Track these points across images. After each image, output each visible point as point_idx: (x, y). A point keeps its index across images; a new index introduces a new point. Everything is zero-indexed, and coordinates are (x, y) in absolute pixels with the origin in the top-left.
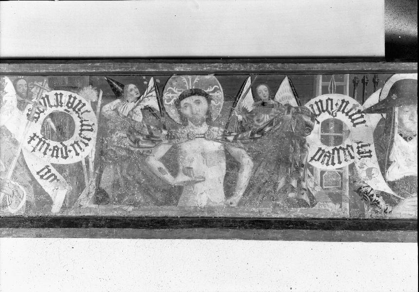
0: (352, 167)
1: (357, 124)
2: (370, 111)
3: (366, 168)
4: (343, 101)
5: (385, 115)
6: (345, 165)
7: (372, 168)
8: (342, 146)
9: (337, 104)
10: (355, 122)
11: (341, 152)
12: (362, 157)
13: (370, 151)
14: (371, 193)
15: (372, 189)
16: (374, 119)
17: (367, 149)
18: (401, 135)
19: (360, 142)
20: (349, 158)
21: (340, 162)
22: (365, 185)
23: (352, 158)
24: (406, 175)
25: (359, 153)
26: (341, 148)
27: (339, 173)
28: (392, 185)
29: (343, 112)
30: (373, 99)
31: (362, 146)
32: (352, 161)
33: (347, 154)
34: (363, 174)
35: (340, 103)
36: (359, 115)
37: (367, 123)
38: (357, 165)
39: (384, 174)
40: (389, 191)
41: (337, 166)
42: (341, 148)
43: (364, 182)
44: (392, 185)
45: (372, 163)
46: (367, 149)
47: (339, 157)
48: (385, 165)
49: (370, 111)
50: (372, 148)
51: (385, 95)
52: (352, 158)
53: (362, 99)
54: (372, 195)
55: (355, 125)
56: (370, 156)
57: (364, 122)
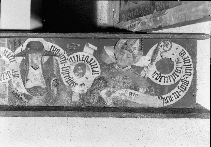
0: (10, 82)
1: (12, 61)
2: (18, 55)
3: (16, 82)
4: (5, 51)
5: (24, 58)
6: (7, 81)
7: (19, 82)
8: (5, 71)
9: (2, 52)
10: (11, 60)
11: (5, 74)
12: (15, 77)
13: (18, 74)
14: (19, 94)
15: (19, 92)
16: (20, 59)
17: (17, 73)
18: (32, 67)
19: (14, 70)
20: (8, 77)
21: (4, 80)
22: (16, 90)
23: (10, 77)
24: (35, 86)
25: (13, 75)
26: (4, 73)
27: (4, 84)
28: (29, 90)
29: (5, 56)
30: (19, 50)
31: (15, 72)
32: (9, 79)
33: (8, 75)
34: (15, 85)
35: (3, 52)
36: (13, 57)
37: (16, 61)
38: (12, 81)
39: (25, 86)
40: (27, 93)
41: (3, 81)
42: (4, 73)
43: (15, 89)
44: (29, 90)
45: (19, 80)
46: (17, 73)
47: (4, 77)
48: (25, 81)
49: (18, 55)
50: (19, 73)
51: (24, 48)
52: (10, 77)
53: (14, 49)
54: (19, 95)
55: (11, 62)
56: (18, 77)
57: (15, 60)
